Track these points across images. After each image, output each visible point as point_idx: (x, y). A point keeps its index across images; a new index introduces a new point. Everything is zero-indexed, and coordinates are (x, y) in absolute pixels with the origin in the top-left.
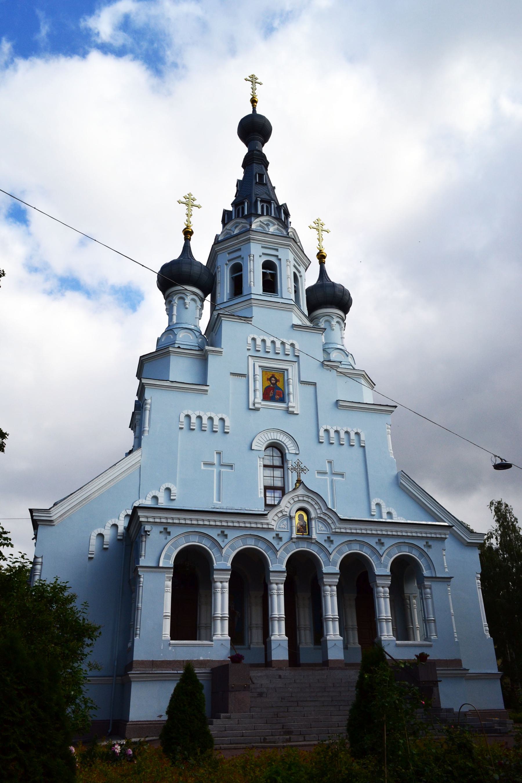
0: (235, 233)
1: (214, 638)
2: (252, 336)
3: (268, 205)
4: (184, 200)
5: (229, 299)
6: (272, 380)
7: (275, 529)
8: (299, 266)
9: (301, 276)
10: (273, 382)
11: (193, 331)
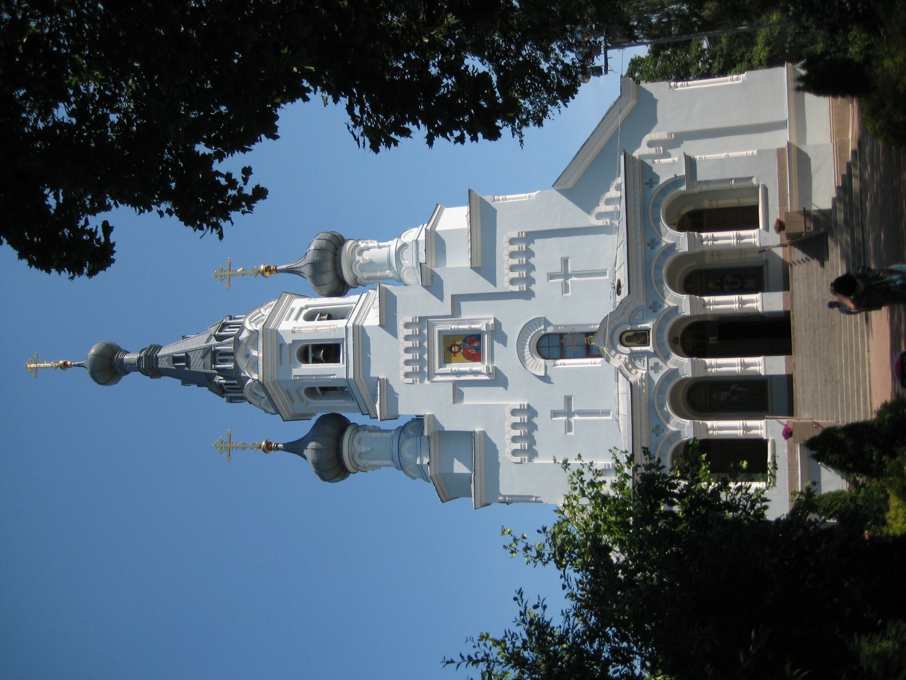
0: (264, 395)
1: (765, 438)
2: (402, 378)
3: (218, 355)
4: (225, 453)
5: (353, 400)
6: (455, 350)
7: (645, 371)
8: (293, 310)
9: (307, 307)
10: (457, 349)
11: (400, 444)
